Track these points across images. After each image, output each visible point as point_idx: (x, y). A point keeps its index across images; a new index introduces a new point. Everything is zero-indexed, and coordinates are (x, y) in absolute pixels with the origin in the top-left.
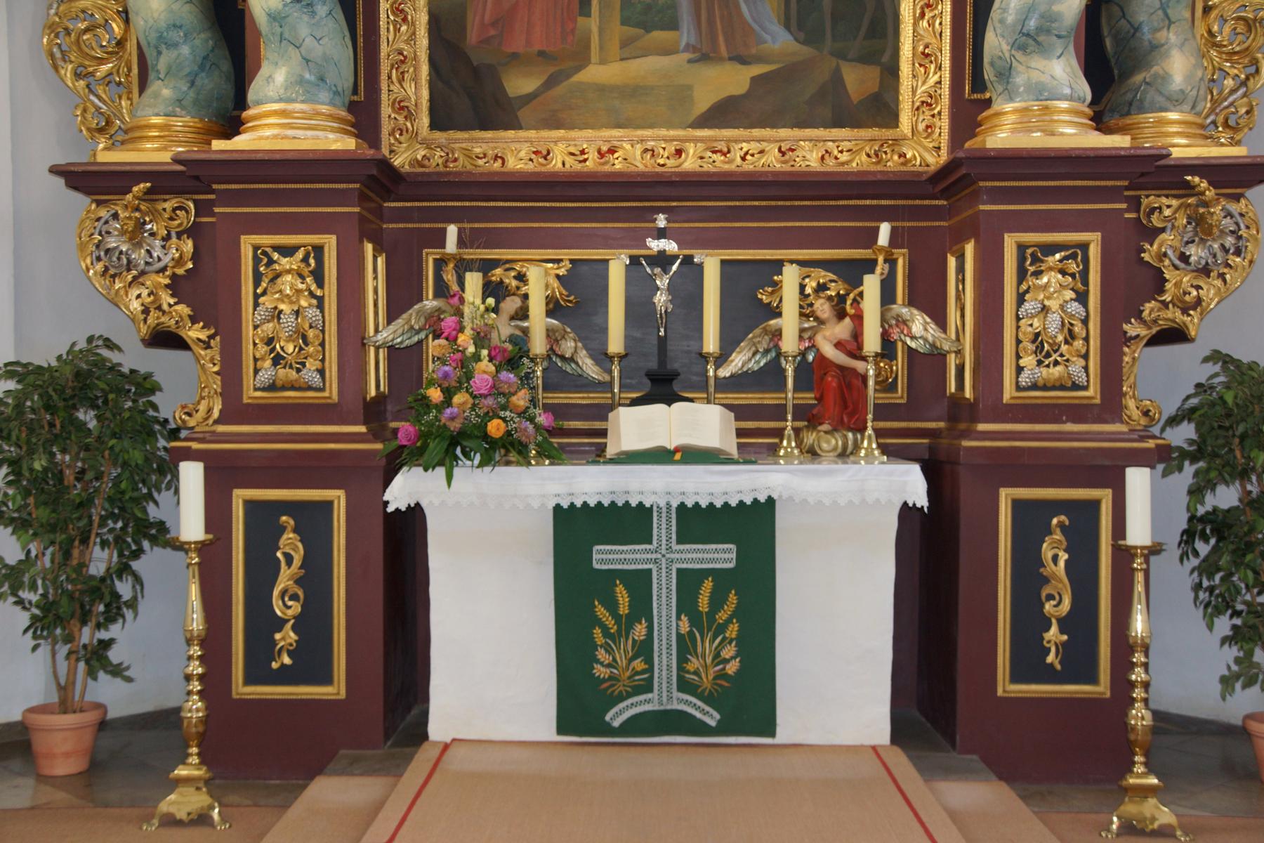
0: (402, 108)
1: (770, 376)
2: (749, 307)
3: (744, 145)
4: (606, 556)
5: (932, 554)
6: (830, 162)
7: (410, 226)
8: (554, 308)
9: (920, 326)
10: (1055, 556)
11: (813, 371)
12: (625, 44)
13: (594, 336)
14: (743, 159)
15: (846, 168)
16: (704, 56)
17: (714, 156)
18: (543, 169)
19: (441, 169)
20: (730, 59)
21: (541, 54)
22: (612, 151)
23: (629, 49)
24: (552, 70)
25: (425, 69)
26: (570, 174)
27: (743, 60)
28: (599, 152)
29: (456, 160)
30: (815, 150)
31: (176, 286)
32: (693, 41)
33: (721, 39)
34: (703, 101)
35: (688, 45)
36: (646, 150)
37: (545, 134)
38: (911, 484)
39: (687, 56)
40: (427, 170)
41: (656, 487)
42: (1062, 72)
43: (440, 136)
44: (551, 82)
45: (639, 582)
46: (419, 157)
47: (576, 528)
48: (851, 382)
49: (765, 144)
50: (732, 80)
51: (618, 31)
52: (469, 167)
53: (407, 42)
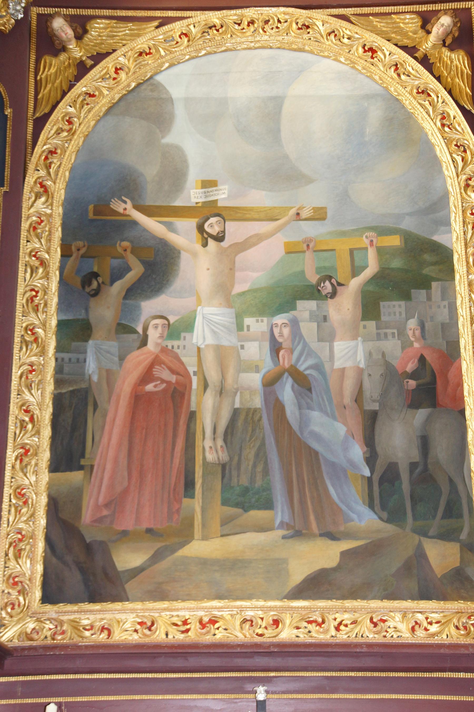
0: (15, 584)
3: (337, 615)
6: (420, 633)
7: (12, 702)
12: (225, 522)
14: (337, 629)
15: (436, 640)
16: (298, 533)
17: (310, 627)
18: (147, 640)
19: (49, 641)
20: (321, 535)
21: (149, 531)
22: (213, 622)
23: (229, 527)
24: (158, 545)
25: (41, 545)
26: (172, 646)
27: (332, 536)
28: (201, 622)
29: (63, 633)
32: (286, 519)
33: (312, 517)
34: (298, 573)
35: (282, 523)
36: (245, 621)
37: (150, 605)
39: (281, 532)
40: (34, 644)
43: (51, 610)
44: (156, 557)
46: (29, 631)
49: (357, 615)
50: (324, 555)
51: (219, 510)
52: (76, 639)
53: (26, 522)
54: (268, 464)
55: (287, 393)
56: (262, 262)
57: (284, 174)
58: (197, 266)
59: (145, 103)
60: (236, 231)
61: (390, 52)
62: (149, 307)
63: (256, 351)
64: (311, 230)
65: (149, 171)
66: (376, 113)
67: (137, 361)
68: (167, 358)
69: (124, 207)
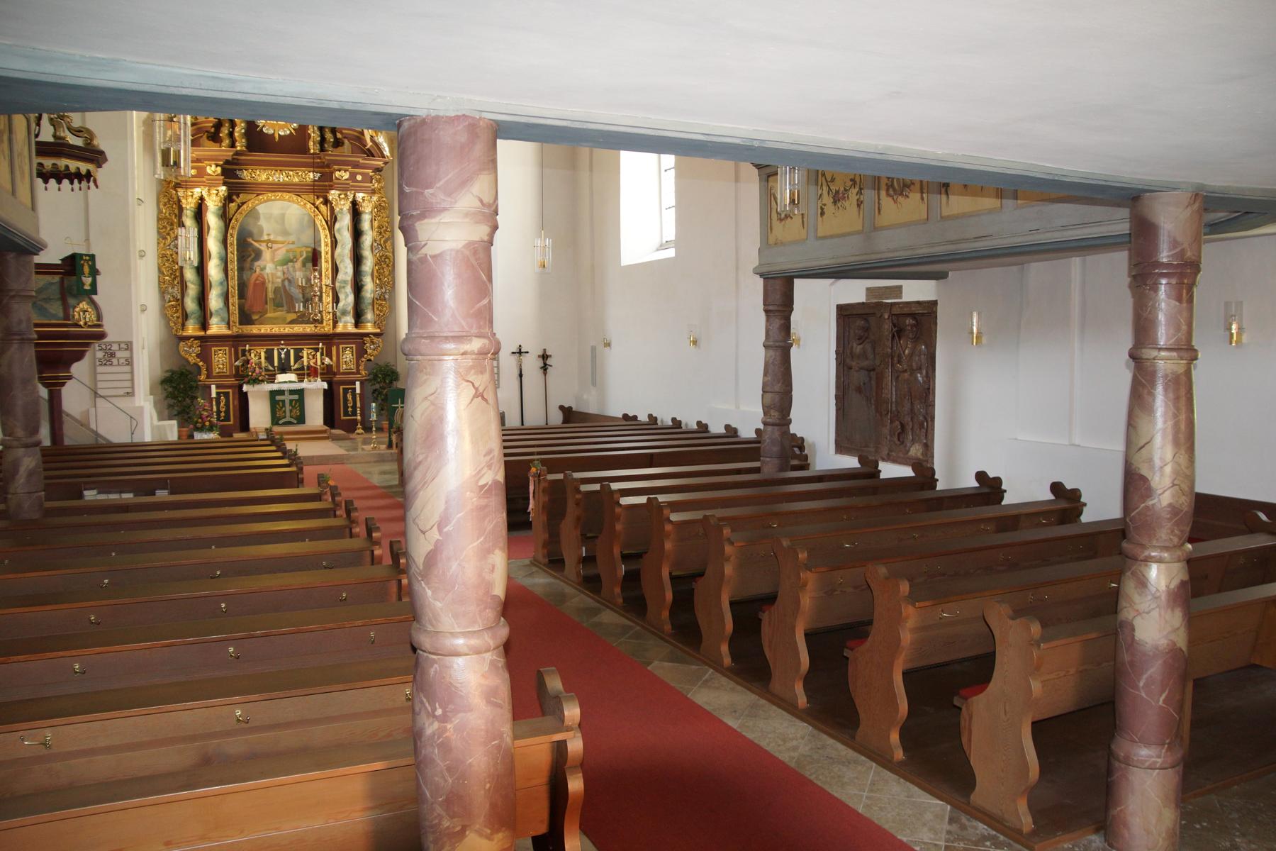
1: (302, 368)
2: (298, 358)
4: (278, 398)
5: (329, 396)
8: (266, 358)
9: (327, 361)
10: (349, 397)
11: (309, 367)
13: (273, 365)
16: (288, 312)
23: (275, 311)
30: (309, 329)
31: (198, 356)
34: (289, 320)
38: (325, 385)
41: (285, 387)
42: (350, 319)
45: (283, 401)
47: (273, 394)
48: (316, 369)
54: (284, 299)
55: (286, 283)
56: (281, 254)
57: (285, 233)
58: (267, 255)
59: (253, 213)
60: (275, 246)
61: (309, 205)
62: (256, 264)
63: (280, 274)
64: (291, 246)
65: (255, 231)
66: (306, 218)
67: (254, 276)
68: (261, 276)
69: (250, 240)
